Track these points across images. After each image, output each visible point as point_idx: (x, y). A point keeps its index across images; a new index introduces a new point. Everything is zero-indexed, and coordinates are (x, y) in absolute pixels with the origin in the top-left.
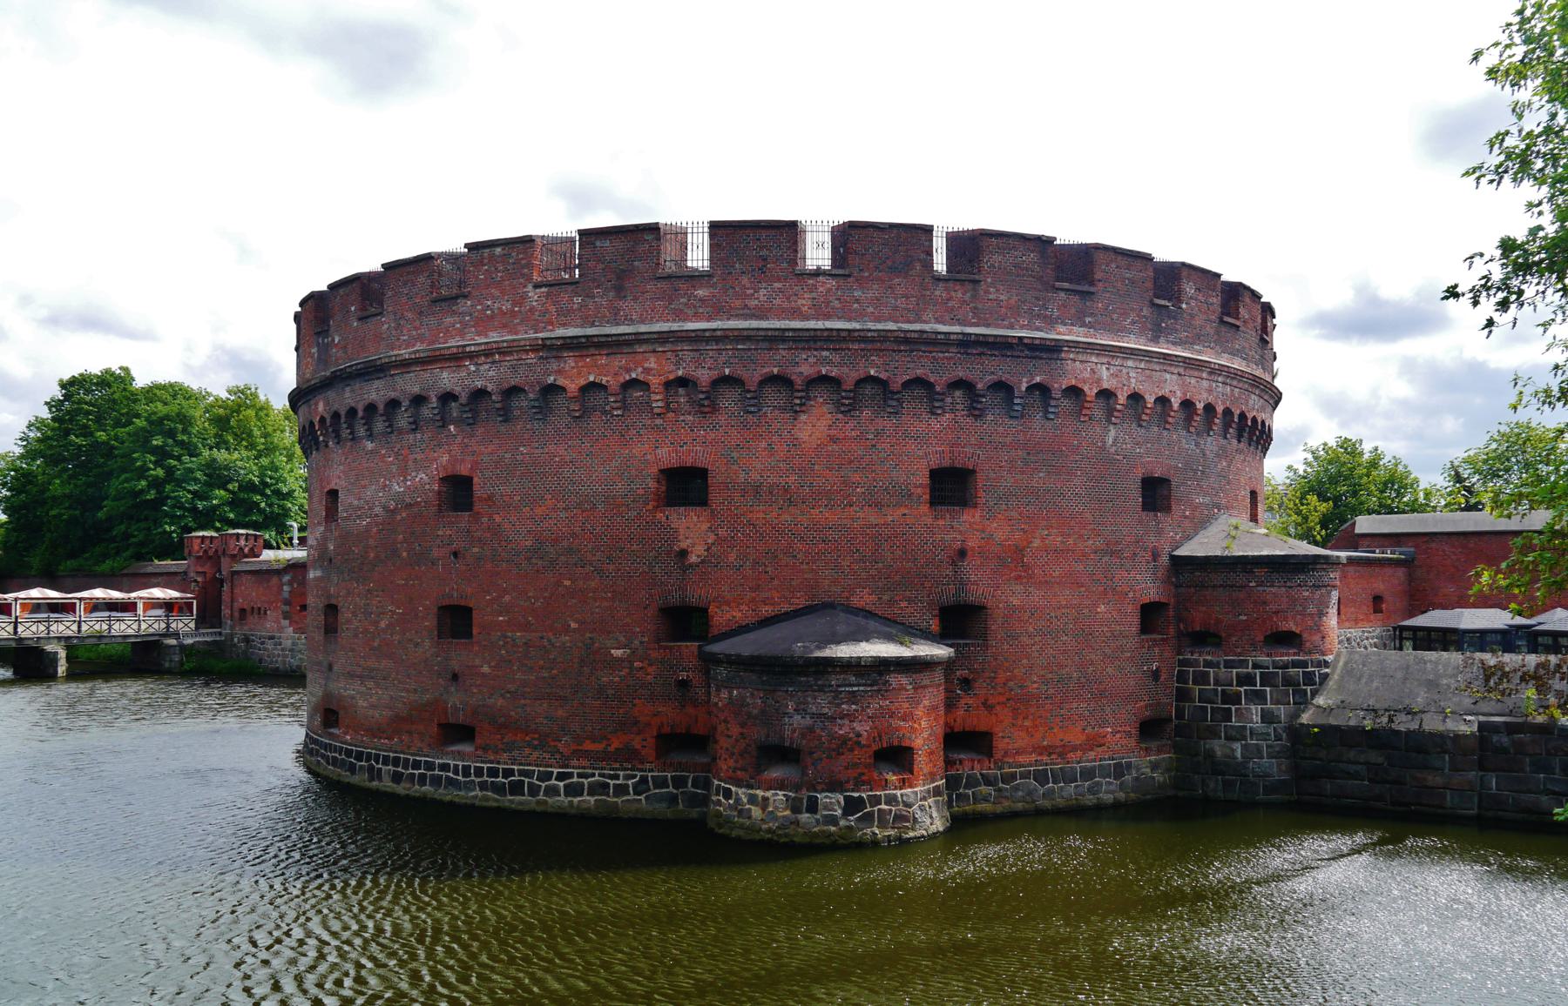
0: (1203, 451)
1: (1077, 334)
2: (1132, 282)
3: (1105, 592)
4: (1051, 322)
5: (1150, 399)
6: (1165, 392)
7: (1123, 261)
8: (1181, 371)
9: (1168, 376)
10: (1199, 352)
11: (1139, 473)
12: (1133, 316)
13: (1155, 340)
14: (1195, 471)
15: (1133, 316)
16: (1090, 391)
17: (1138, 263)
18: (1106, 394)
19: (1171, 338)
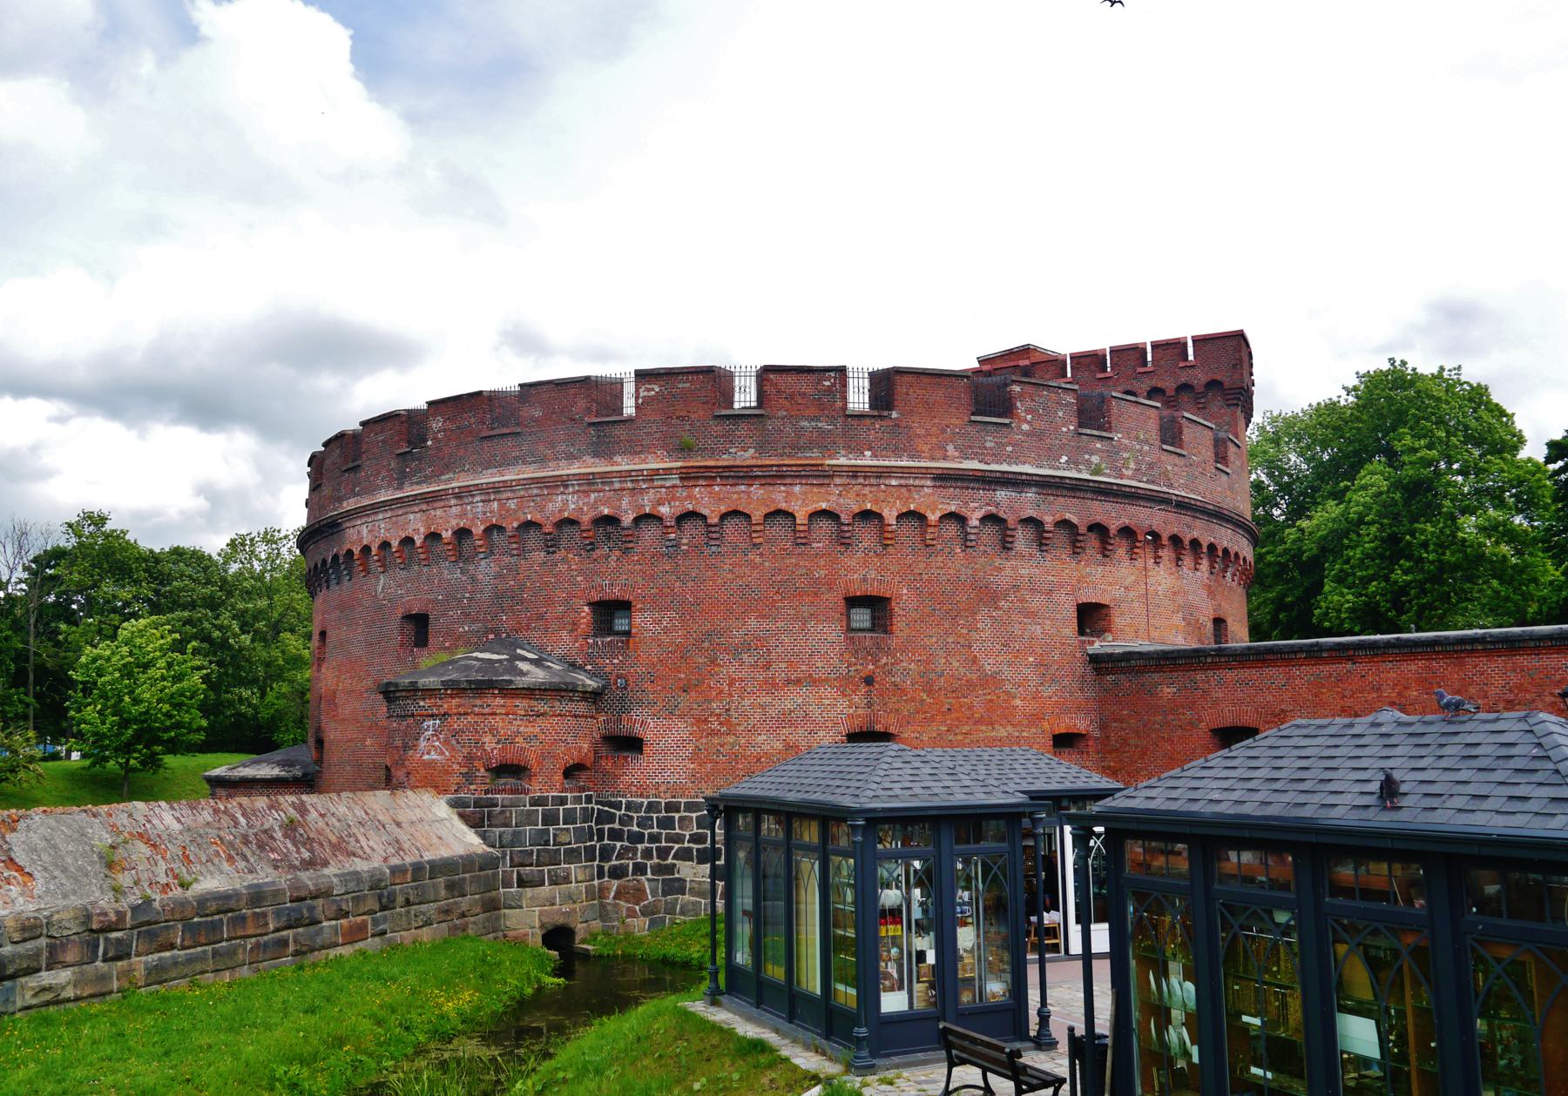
0: (474, 579)
1: (350, 504)
2: (384, 442)
3: (370, 728)
4: (340, 500)
5: (395, 544)
6: (409, 532)
7: (378, 427)
8: (424, 507)
9: (411, 516)
10: (449, 480)
11: (400, 612)
12: (384, 473)
13: (400, 487)
14: (460, 601)
15: (384, 473)
16: (356, 551)
17: (389, 424)
18: (366, 549)
19: (415, 479)
